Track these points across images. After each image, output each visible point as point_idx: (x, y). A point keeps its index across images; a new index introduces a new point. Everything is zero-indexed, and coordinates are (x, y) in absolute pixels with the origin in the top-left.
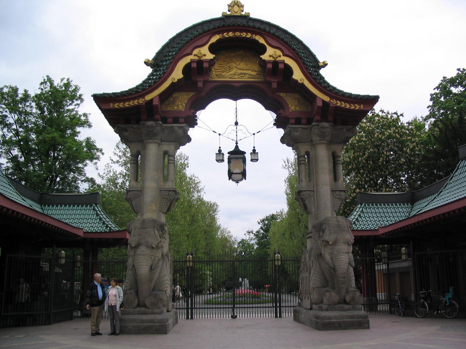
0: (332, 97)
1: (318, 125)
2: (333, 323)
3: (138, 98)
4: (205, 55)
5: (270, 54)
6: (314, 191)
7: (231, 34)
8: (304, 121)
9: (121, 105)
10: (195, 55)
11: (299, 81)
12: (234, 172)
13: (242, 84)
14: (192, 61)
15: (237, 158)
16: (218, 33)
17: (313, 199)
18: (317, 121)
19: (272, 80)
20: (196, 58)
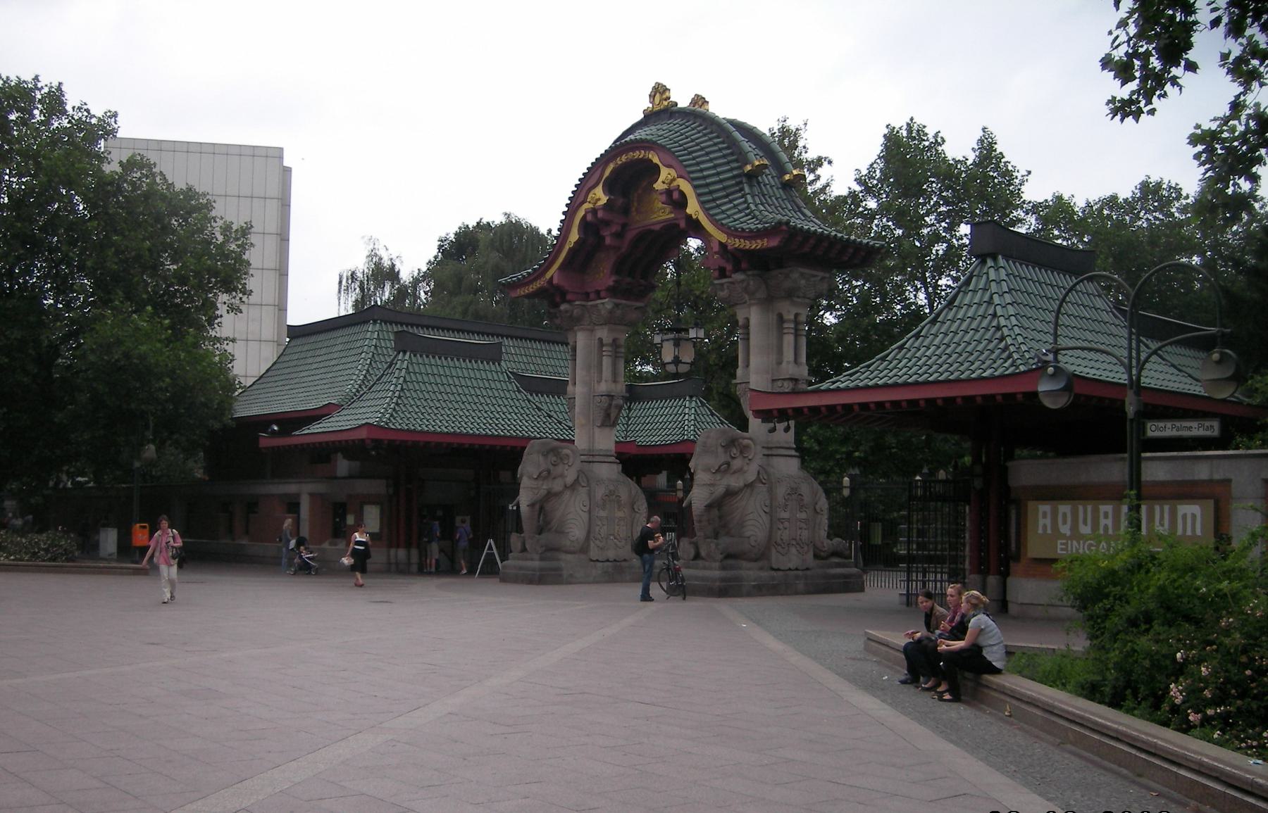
4: (599, 199)
7: (624, 158)
14: (587, 212)
20: (591, 206)
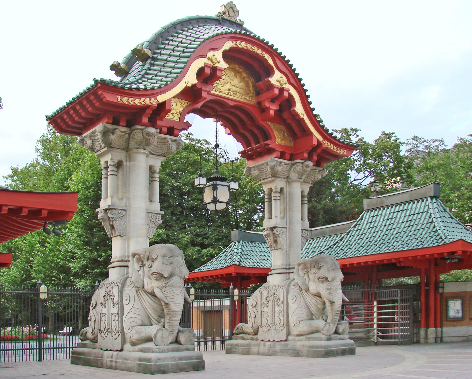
13: (236, 103)
15: (223, 185)
17: (285, 236)
19: (271, 107)
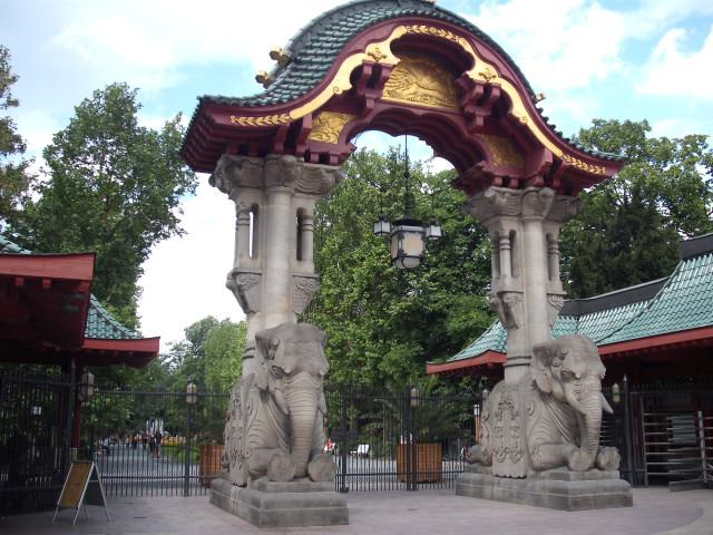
0: (565, 151)
1: (537, 192)
2: (586, 499)
3: (279, 112)
4: (385, 57)
5: (479, 71)
6: (522, 293)
7: (423, 29)
8: (514, 183)
9: (250, 120)
10: (369, 54)
11: (521, 120)
12: (409, 254)
13: (426, 112)
14: (365, 64)
15: (413, 232)
16: (405, 23)
18: (537, 186)
19: (477, 113)
20: (371, 59)
